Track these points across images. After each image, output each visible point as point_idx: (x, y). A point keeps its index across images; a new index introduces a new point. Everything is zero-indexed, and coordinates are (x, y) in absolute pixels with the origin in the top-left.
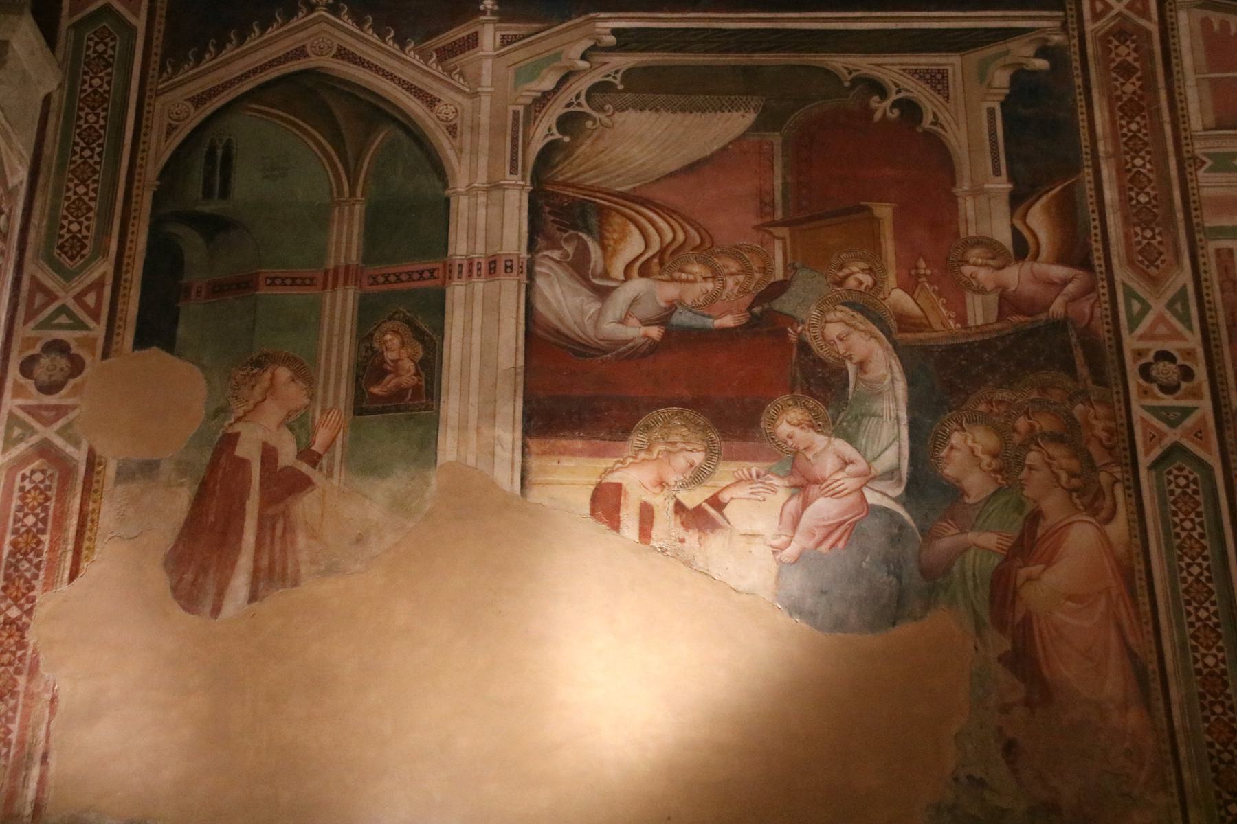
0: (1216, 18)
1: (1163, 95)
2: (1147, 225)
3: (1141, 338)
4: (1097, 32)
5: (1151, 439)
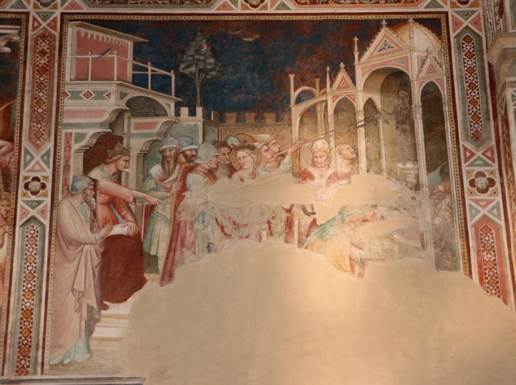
0: (83, 31)
1: (56, 65)
2: (39, 122)
3: (29, 171)
4: (33, 36)
5: (23, 214)
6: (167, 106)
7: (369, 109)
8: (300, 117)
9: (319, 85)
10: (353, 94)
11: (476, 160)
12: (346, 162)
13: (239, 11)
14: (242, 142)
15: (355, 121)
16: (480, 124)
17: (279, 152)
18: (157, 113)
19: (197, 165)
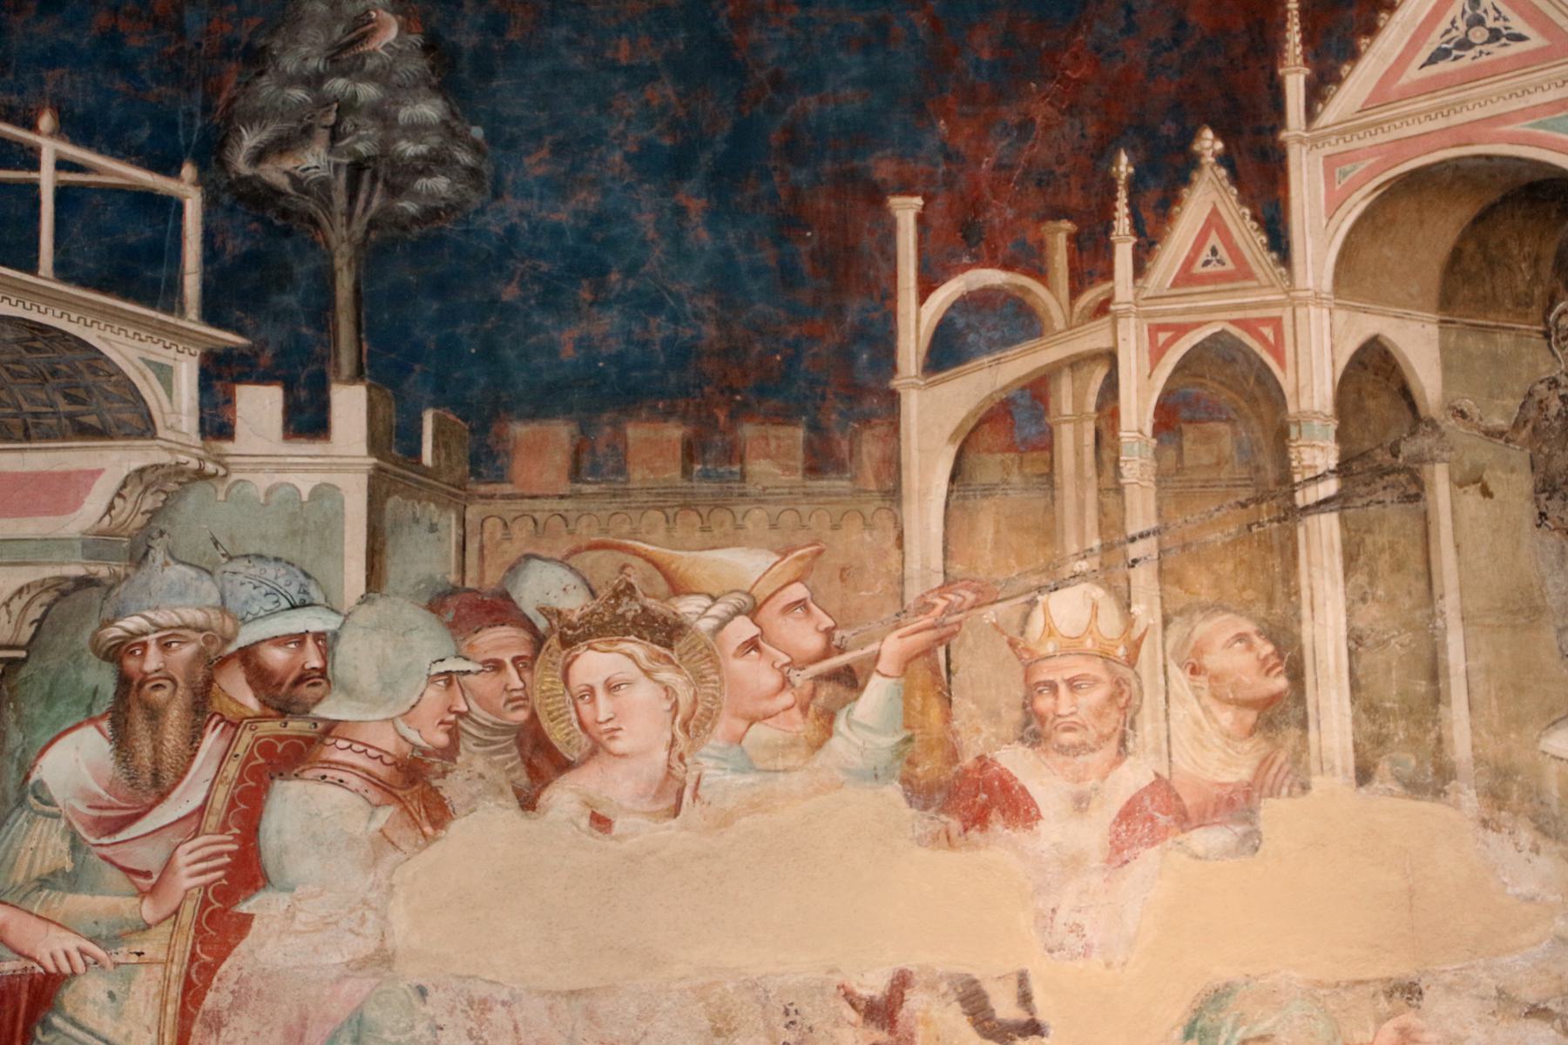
6: (151, 376)
7: (1370, 404)
8: (952, 451)
9: (1071, 262)
10: (1274, 312)
12: (1226, 717)
14: (604, 593)
17: (826, 654)
18: (92, 420)
19: (330, 728)
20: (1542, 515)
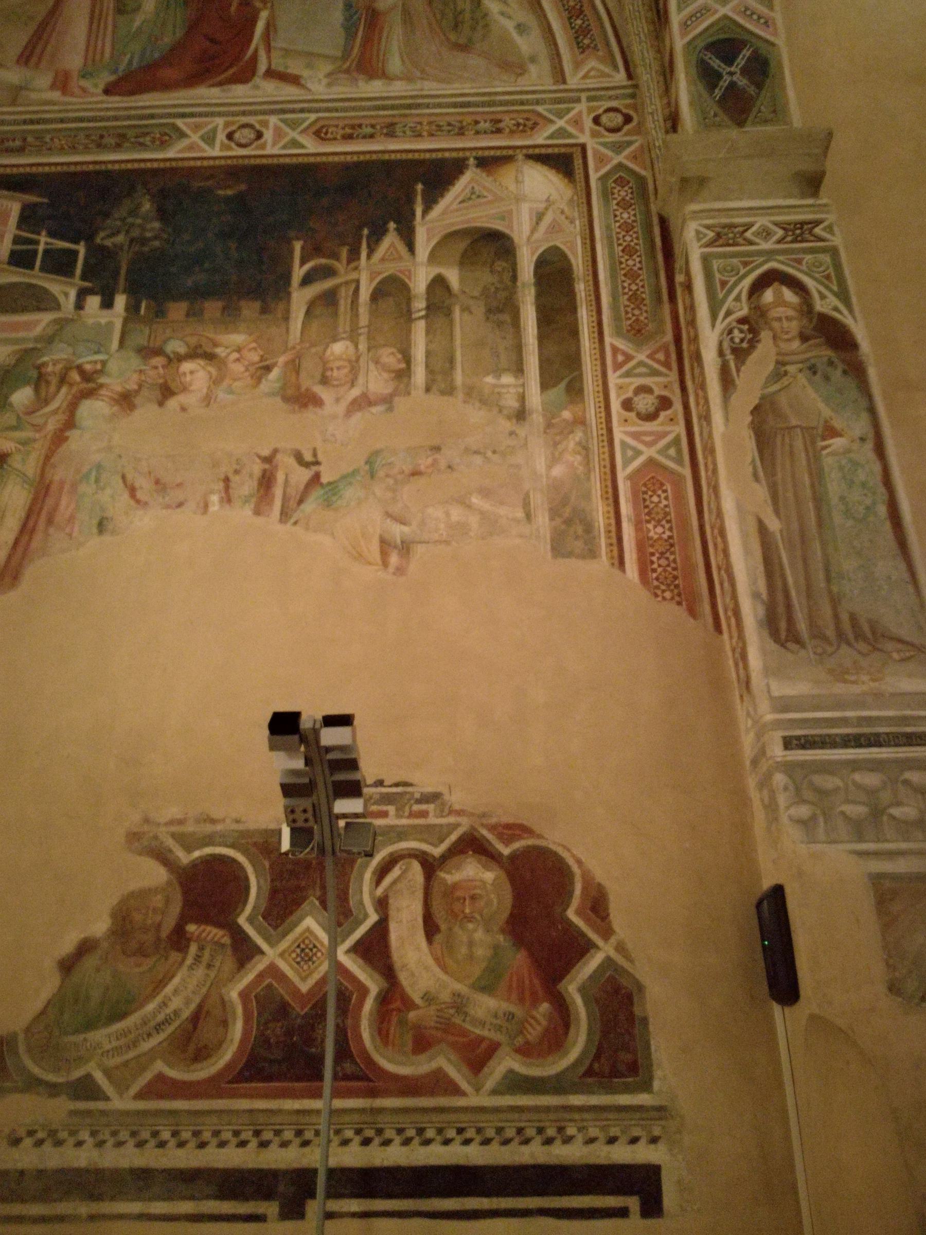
11: (634, 367)
13: (216, 152)
15: (409, 312)
16: (644, 308)
19: (101, 386)
20: (488, 318)
